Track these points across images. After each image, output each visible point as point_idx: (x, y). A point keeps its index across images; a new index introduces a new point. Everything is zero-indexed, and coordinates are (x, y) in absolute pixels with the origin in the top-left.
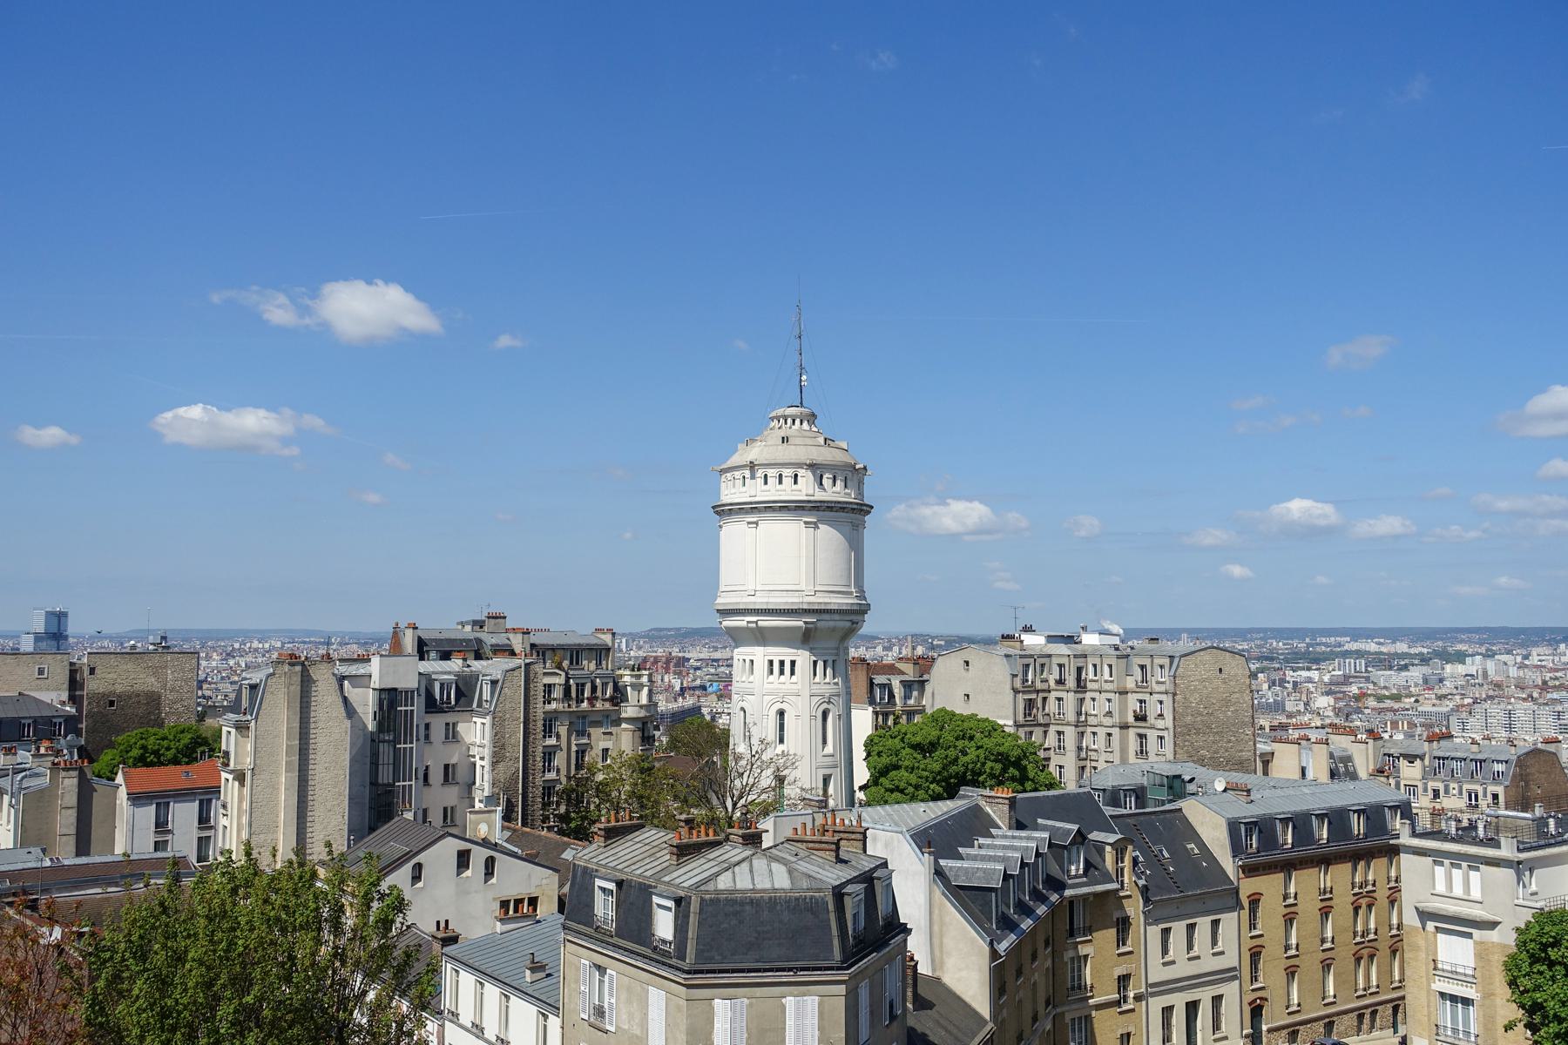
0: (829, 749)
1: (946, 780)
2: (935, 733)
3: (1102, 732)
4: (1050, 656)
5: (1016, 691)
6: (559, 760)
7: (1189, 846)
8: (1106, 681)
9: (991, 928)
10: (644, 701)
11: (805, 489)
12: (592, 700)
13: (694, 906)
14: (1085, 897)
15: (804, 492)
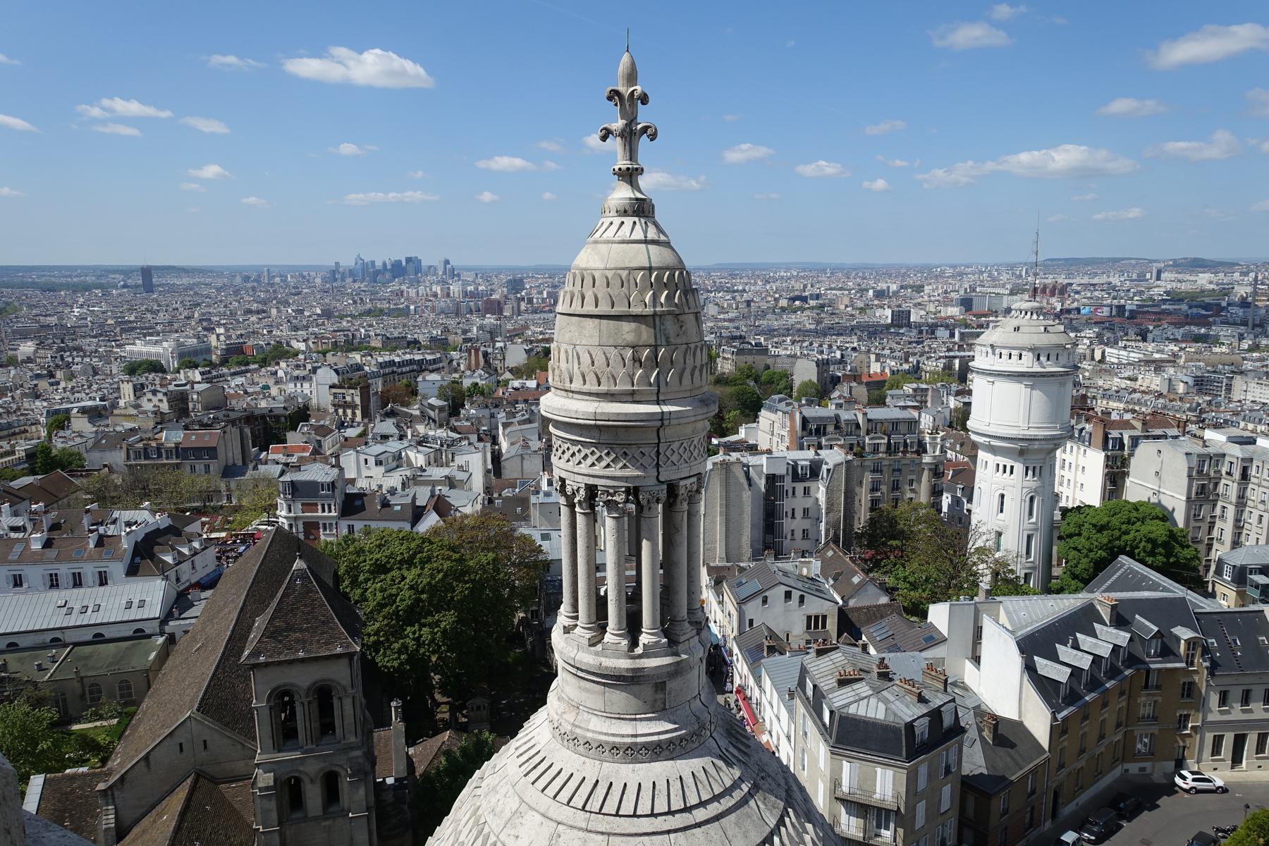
0: (1034, 520)
1: (1112, 549)
2: (1106, 519)
3: (1256, 514)
4: (1224, 455)
5: (1190, 476)
6: (884, 488)
7: (1260, 638)
8: (1264, 480)
9: (1057, 703)
10: (937, 453)
11: (1027, 364)
12: (904, 452)
13: (837, 718)
14: (1159, 670)
15: (1026, 365)
